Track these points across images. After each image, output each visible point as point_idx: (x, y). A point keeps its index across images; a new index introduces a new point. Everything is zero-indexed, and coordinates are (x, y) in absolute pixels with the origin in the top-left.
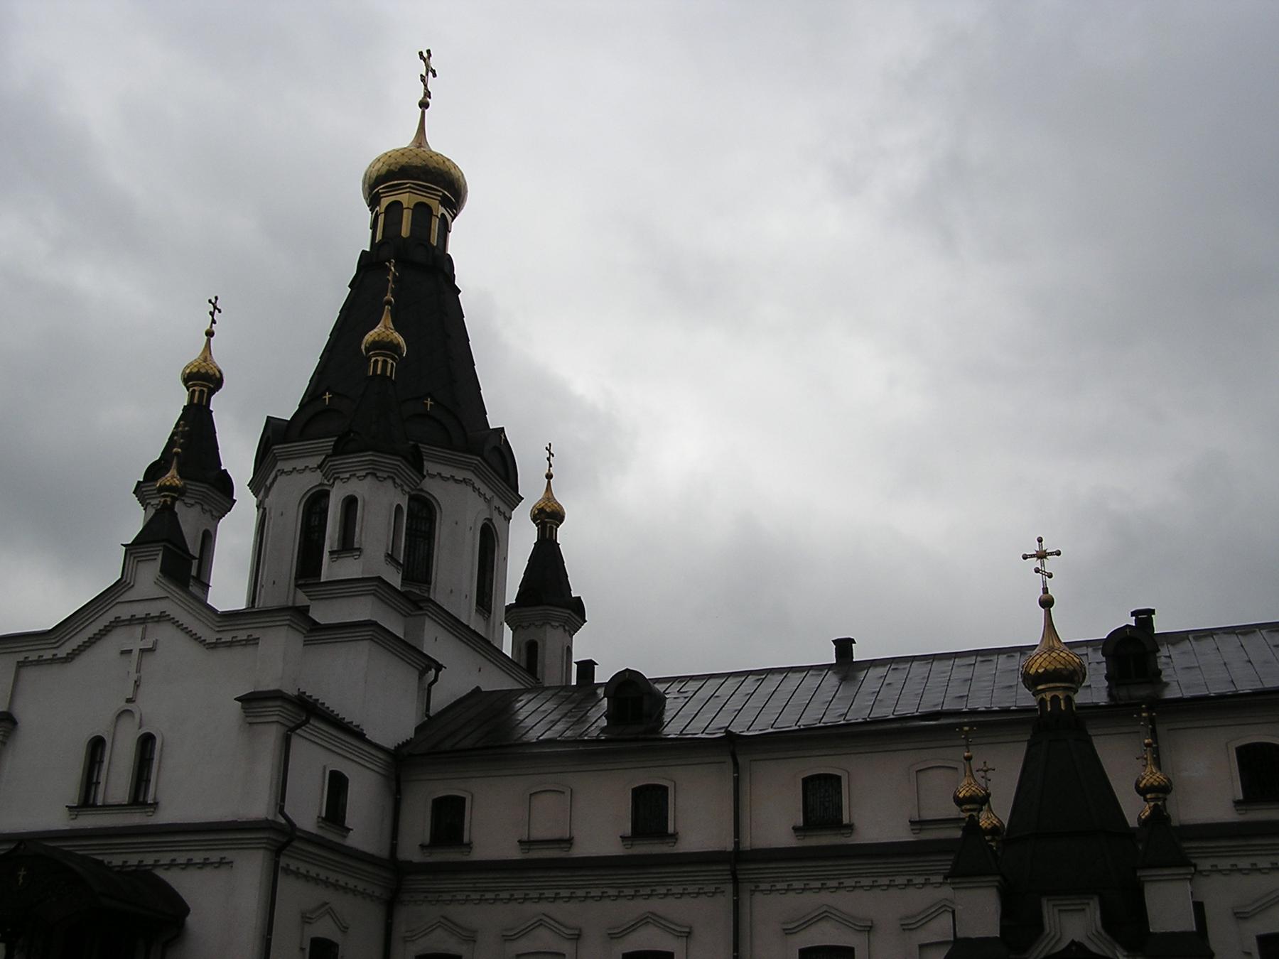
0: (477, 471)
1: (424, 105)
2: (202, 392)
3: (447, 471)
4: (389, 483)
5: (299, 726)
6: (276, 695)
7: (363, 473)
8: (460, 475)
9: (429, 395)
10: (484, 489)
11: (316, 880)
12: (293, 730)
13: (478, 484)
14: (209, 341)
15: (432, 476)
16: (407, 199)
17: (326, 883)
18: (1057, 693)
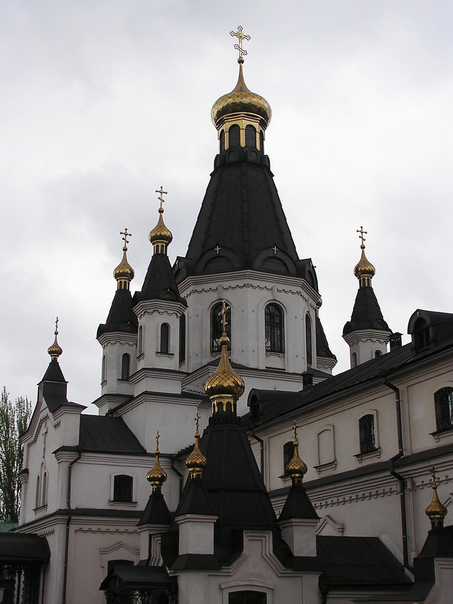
0: (250, 277)
1: (241, 62)
2: (125, 282)
3: (233, 284)
4: (156, 313)
5: (75, 461)
6: (64, 449)
7: (143, 313)
8: (241, 283)
9: (217, 245)
10: (262, 284)
11: (108, 531)
12: (72, 463)
13: (255, 283)
14: (125, 253)
15: (226, 289)
16: (226, 127)
17: (117, 531)
18: (220, 400)
